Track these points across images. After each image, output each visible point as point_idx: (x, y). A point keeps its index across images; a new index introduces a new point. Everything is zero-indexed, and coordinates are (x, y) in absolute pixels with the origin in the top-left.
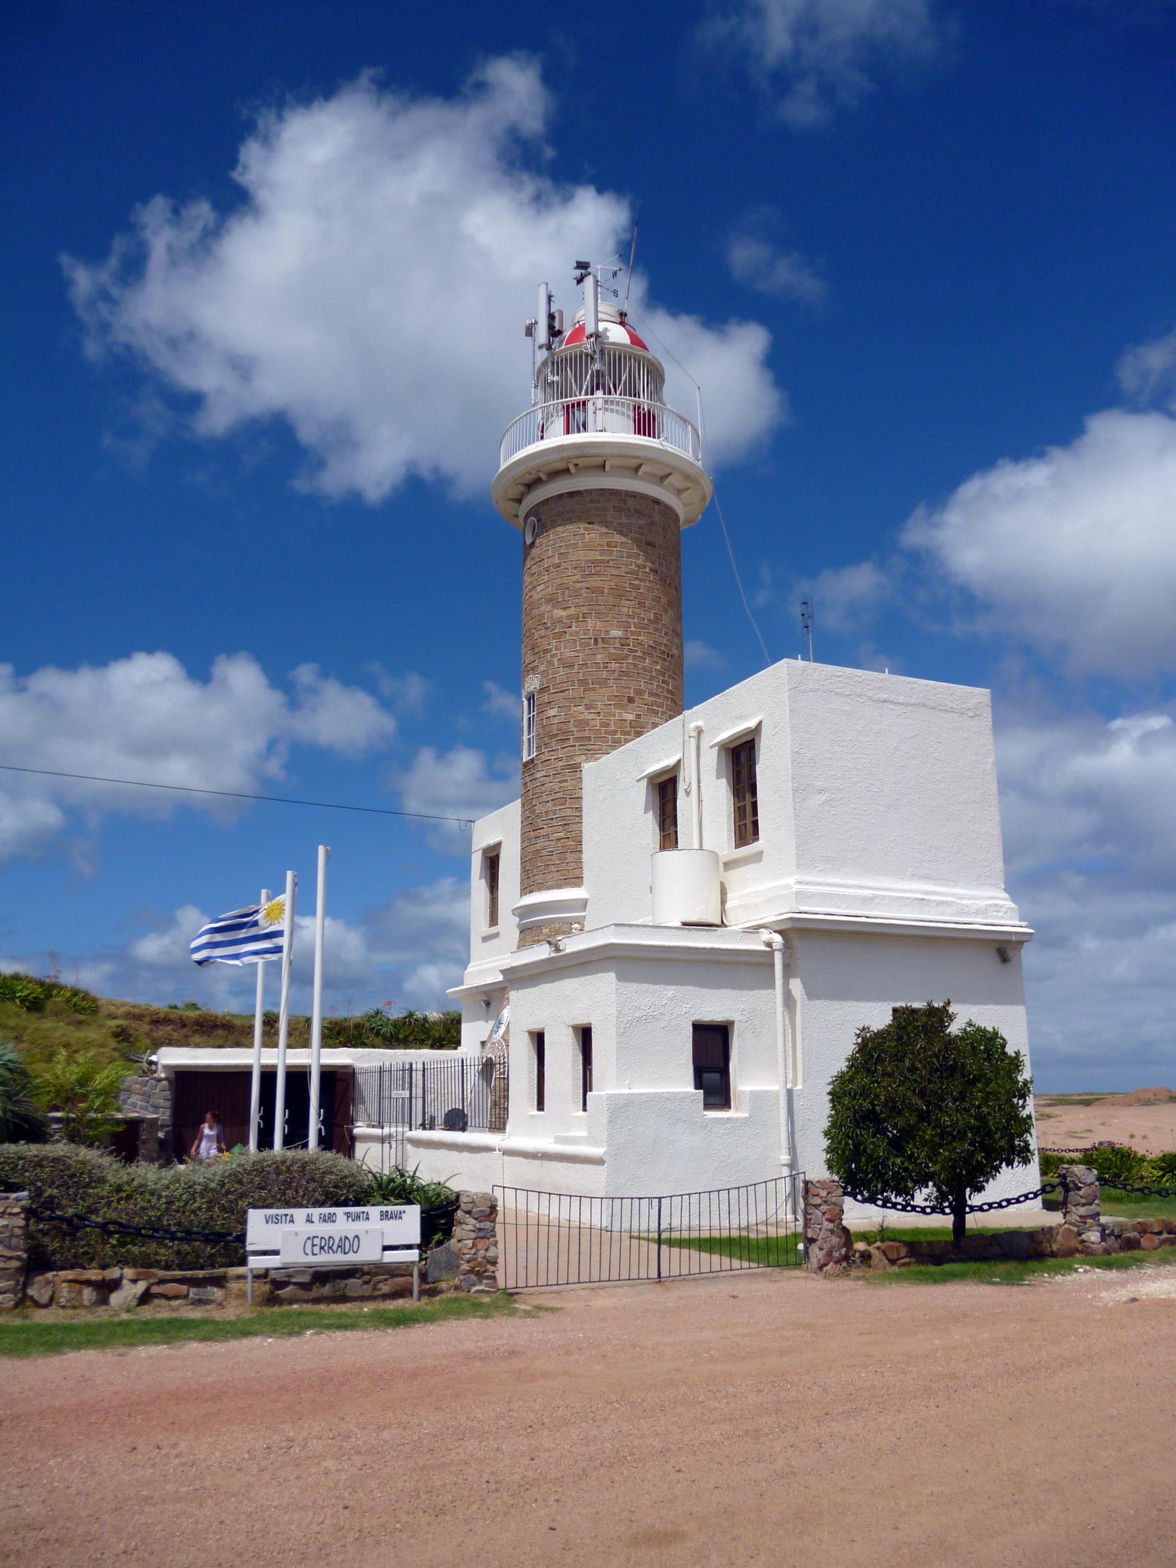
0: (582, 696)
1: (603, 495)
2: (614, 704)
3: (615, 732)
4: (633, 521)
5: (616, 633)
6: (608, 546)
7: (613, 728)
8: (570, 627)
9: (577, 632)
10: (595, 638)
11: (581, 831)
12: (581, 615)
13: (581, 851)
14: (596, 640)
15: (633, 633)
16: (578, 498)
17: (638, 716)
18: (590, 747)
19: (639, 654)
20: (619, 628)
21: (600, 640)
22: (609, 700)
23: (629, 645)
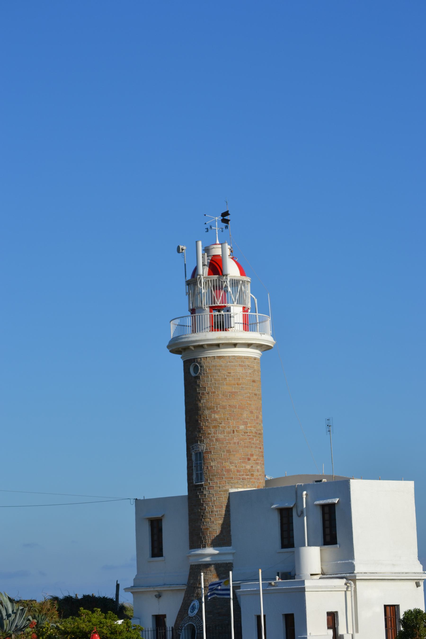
0: (228, 457)
1: (234, 359)
2: (242, 462)
3: (243, 475)
4: (247, 371)
5: (242, 427)
6: (238, 384)
7: (242, 473)
8: (221, 424)
9: (225, 427)
10: (233, 430)
11: (230, 521)
12: (226, 418)
13: (230, 531)
14: (233, 431)
15: (249, 427)
16: (222, 360)
17: (252, 467)
18: (232, 482)
19: (252, 437)
20: (243, 425)
21: (235, 431)
22: (240, 460)
23: (247, 433)
